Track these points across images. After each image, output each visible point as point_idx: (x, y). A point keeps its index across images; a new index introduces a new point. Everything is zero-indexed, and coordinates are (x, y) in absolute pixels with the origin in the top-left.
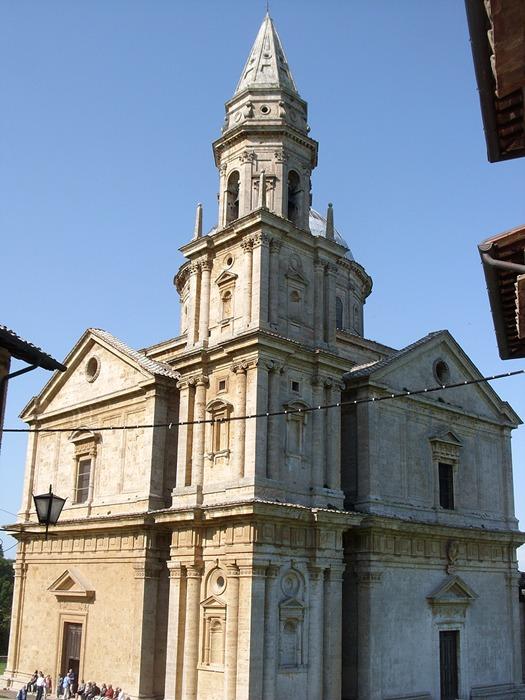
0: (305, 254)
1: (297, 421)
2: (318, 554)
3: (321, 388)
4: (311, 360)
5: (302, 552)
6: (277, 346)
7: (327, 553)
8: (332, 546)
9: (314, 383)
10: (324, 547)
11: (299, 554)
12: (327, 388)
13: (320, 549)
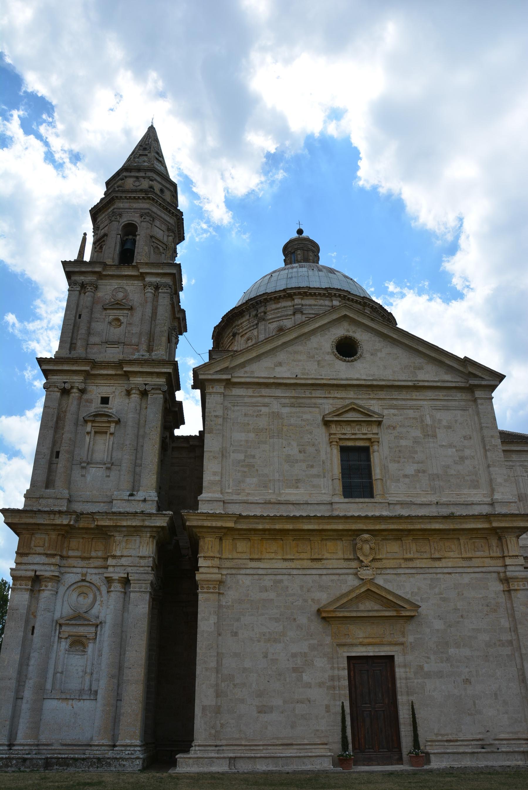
0: (133, 285)
1: (106, 433)
2: (110, 561)
3: (135, 397)
4: (119, 372)
5: (99, 563)
6: (66, 367)
7: (124, 561)
8: (133, 553)
9: (128, 393)
10: (118, 553)
11: (92, 566)
12: (144, 394)
13: (114, 557)
